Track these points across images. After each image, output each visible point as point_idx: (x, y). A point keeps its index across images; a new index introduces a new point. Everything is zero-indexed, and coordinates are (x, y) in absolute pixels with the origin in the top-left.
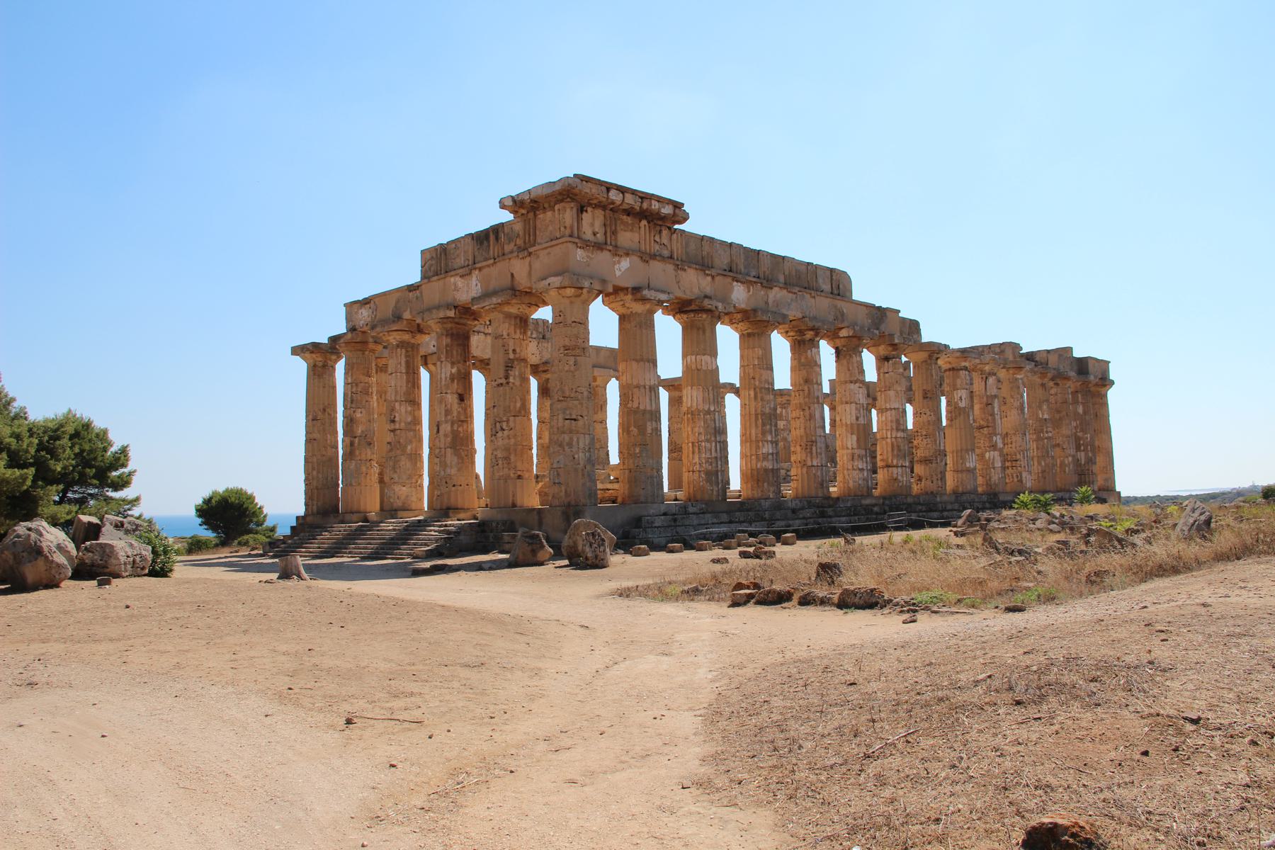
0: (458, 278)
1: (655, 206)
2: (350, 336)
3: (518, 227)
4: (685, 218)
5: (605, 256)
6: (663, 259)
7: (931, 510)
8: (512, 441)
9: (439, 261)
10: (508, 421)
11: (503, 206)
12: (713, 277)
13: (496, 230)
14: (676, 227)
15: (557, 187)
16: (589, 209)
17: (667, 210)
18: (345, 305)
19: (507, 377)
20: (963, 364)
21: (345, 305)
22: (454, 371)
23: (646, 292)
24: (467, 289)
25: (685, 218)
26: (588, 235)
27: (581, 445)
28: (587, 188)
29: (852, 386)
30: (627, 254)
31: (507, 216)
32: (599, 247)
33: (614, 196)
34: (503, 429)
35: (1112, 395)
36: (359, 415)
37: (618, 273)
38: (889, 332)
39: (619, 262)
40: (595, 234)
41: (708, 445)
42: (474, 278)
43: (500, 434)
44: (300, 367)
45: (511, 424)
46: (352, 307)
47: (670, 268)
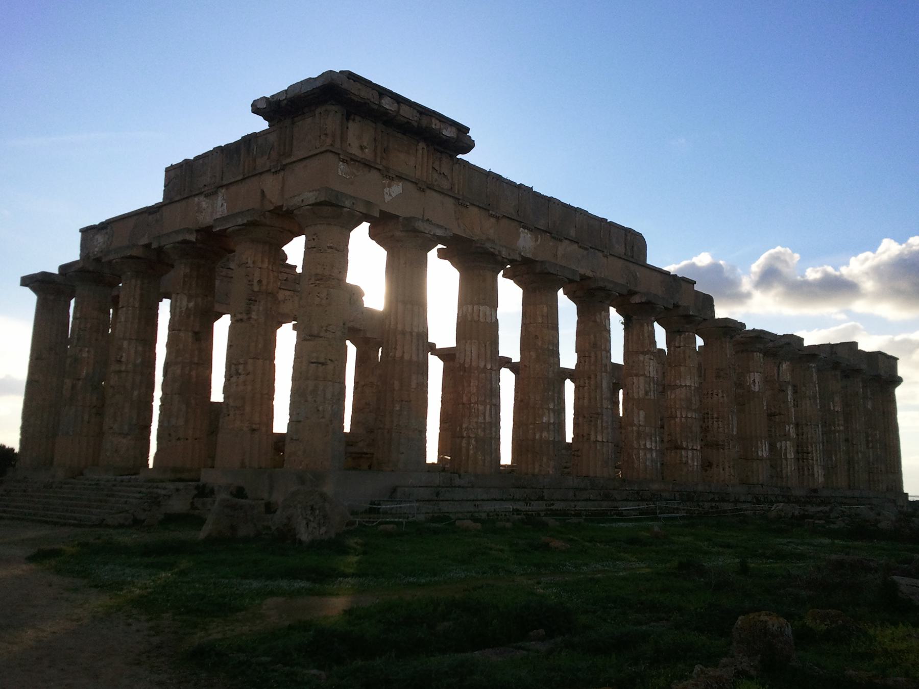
0: (202, 198)
1: (436, 124)
2: (81, 265)
3: (272, 138)
4: (468, 146)
7: (723, 500)
8: (249, 388)
9: (182, 177)
10: (245, 363)
11: (256, 109)
12: (498, 218)
13: (249, 140)
14: (459, 156)
15: (319, 84)
16: (358, 118)
17: (448, 133)
18: (82, 231)
19: (248, 312)
21: (82, 231)
22: (191, 305)
24: (214, 210)
25: (468, 146)
26: (355, 150)
27: (329, 396)
28: (354, 88)
29: (641, 358)
30: (400, 178)
31: (260, 124)
32: (368, 165)
34: (238, 374)
35: (899, 391)
36: (85, 355)
37: (387, 198)
38: (681, 303)
39: (390, 186)
40: (362, 148)
41: (481, 408)
42: (220, 198)
43: (234, 379)
44: (30, 299)
45: (250, 368)
46: (88, 233)
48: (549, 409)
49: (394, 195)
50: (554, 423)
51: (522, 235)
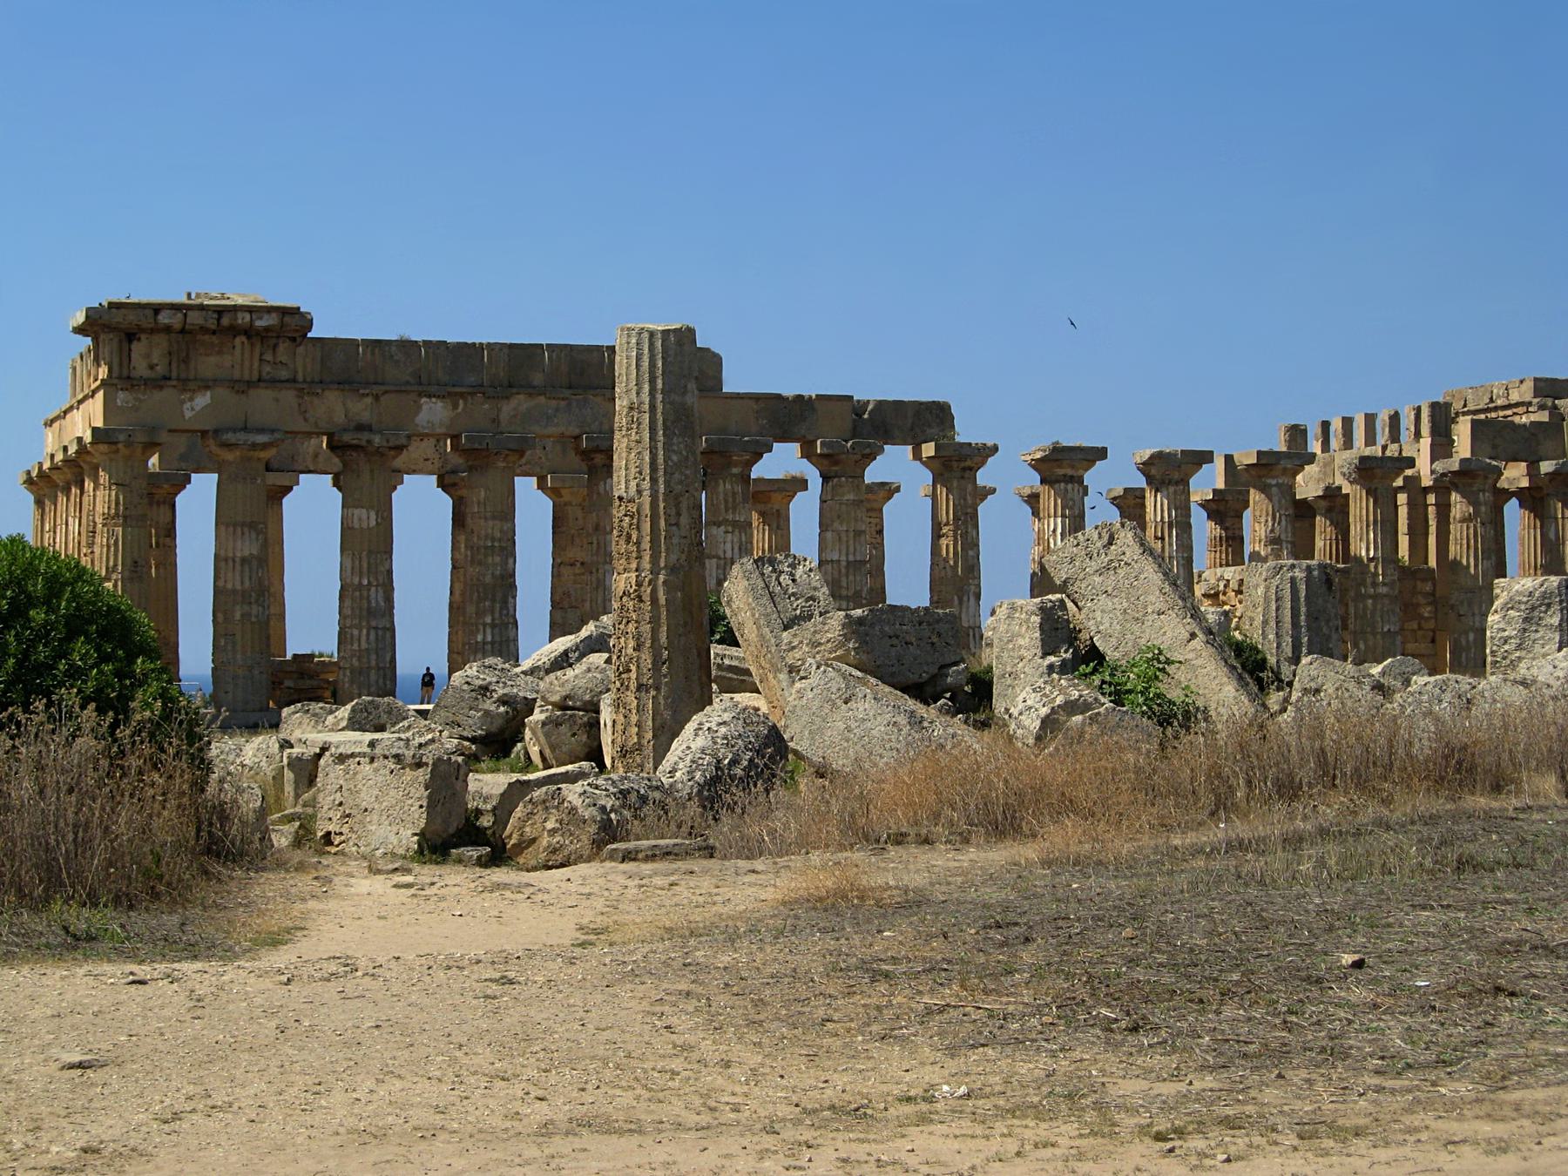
5: (168, 394)
6: (274, 382)
12: (377, 398)
16: (143, 337)
20: (1061, 472)
23: (230, 437)
25: (309, 325)
30: (207, 388)
33: (164, 318)
37: (188, 414)
39: (191, 399)
40: (152, 367)
41: (356, 632)
47: (289, 396)
48: (485, 625)
49: (198, 409)
50: (493, 643)
51: (425, 407)
